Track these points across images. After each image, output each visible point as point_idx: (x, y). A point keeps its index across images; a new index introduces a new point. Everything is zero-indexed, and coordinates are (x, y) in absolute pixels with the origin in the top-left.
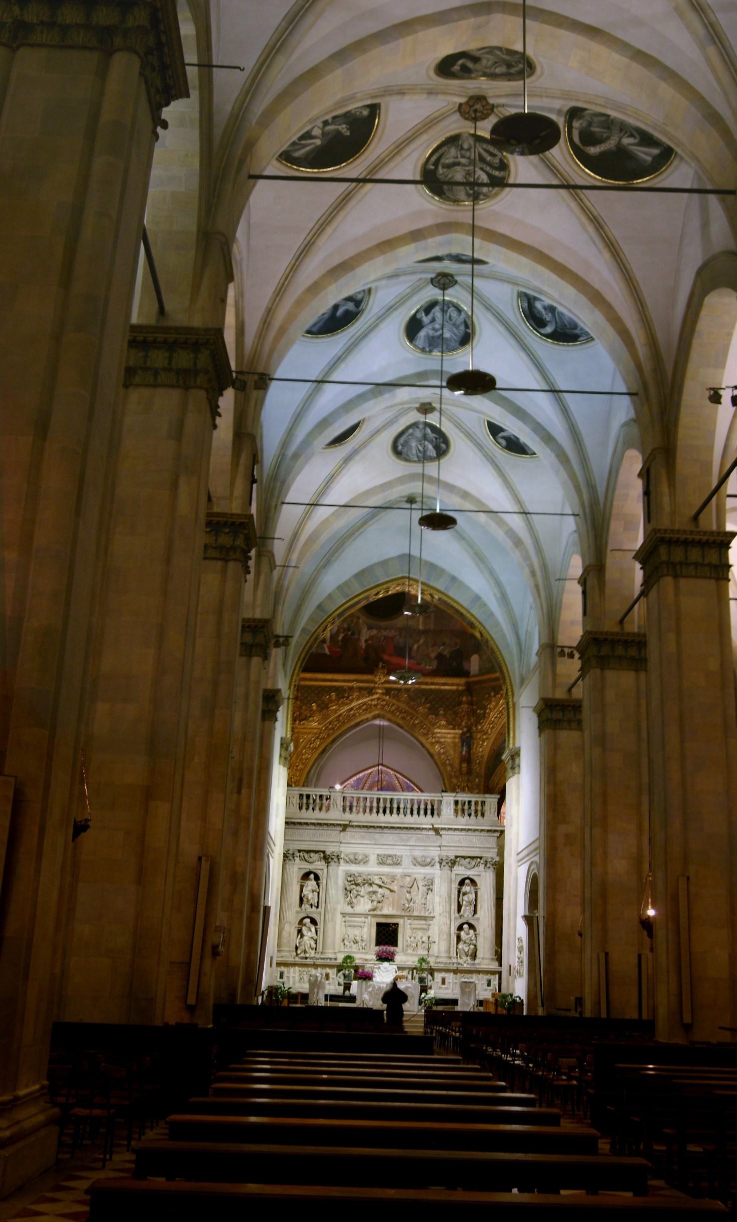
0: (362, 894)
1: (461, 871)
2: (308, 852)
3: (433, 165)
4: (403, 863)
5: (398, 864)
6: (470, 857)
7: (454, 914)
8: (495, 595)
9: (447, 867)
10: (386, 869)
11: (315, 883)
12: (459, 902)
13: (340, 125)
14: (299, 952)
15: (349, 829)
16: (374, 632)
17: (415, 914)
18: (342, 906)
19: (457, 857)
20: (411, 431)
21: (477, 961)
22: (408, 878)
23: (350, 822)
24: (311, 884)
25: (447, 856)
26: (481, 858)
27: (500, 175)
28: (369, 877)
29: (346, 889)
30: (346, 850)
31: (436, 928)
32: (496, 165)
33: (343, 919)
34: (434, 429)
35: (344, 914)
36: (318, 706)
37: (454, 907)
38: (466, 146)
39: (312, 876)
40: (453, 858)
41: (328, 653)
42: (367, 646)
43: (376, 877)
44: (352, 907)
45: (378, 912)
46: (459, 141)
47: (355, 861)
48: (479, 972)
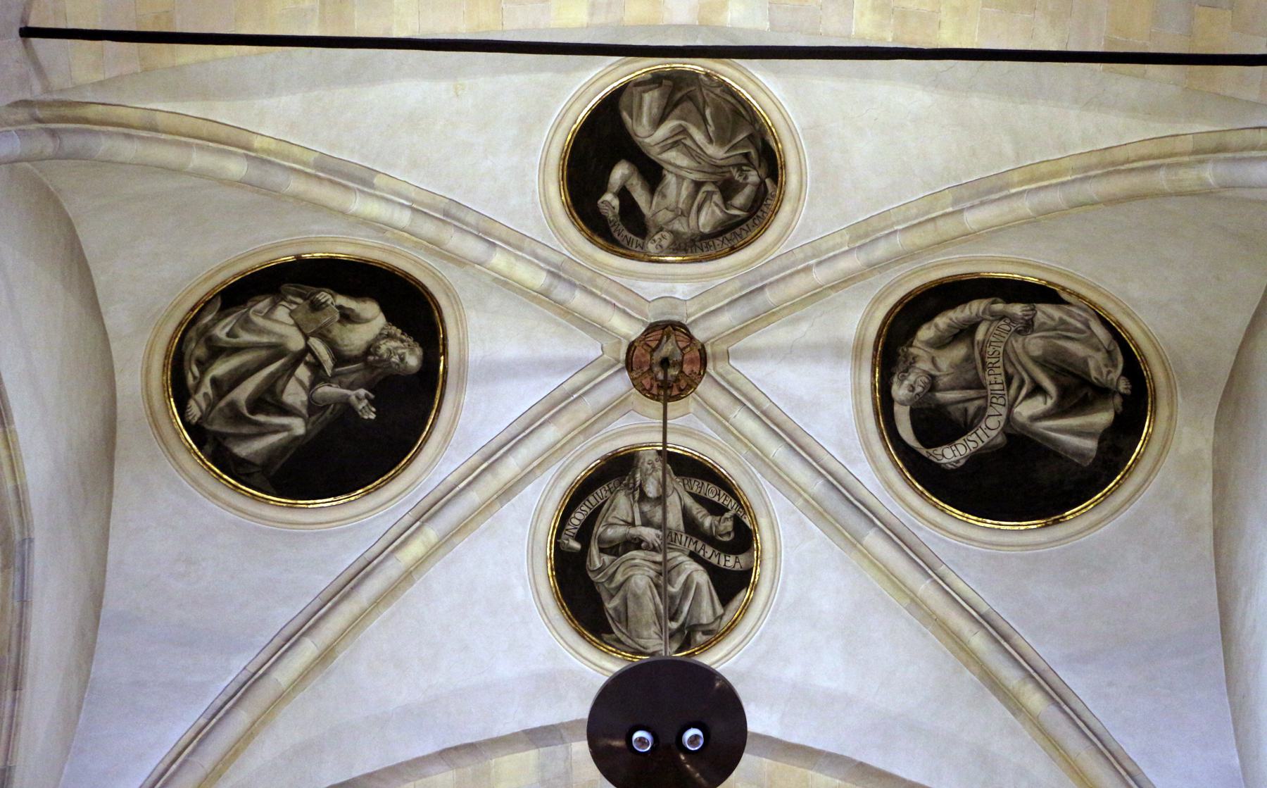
3: (577, 538)
13: (351, 386)
27: (738, 567)
32: (726, 539)
38: (652, 490)
46: (634, 474)
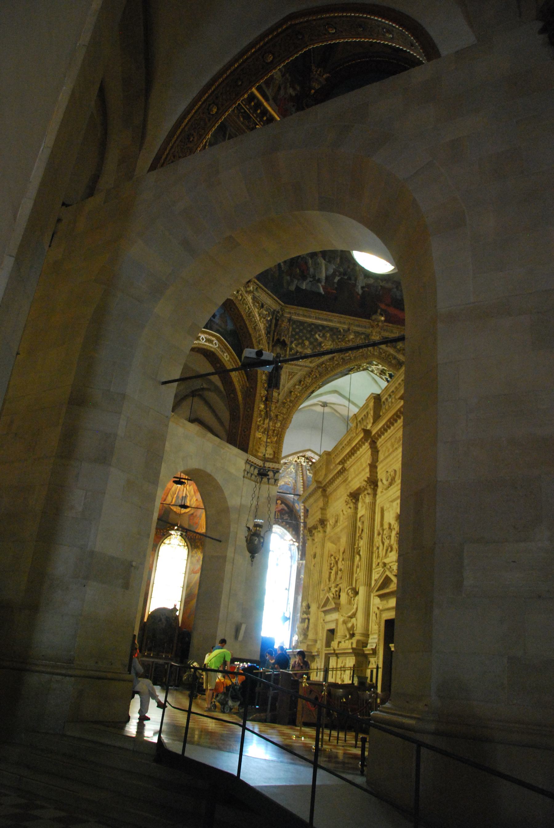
36: (311, 343)
41: (323, 293)
42: (364, 292)
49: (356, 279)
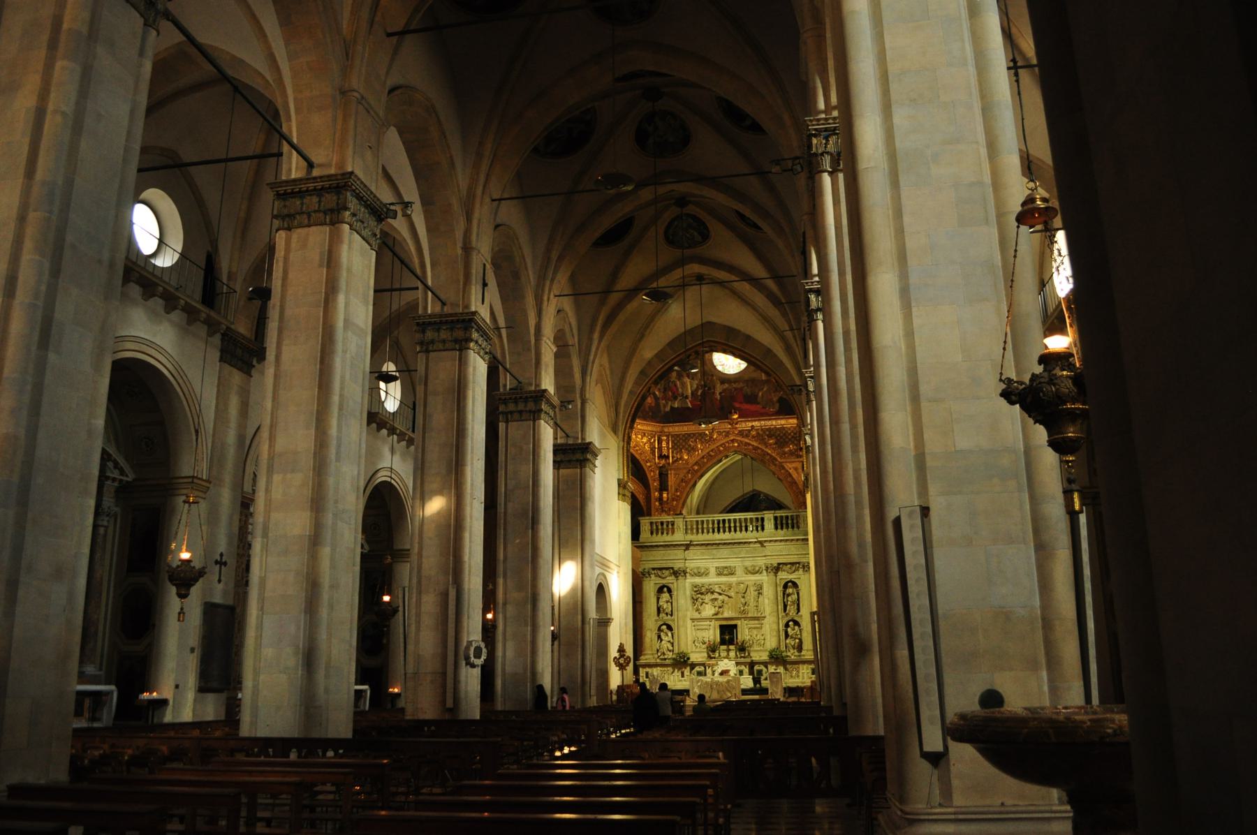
0: (706, 601)
1: (784, 576)
2: (661, 569)
4: (737, 573)
5: (732, 574)
6: (790, 563)
7: (781, 614)
8: (781, 347)
9: (772, 574)
10: (723, 579)
11: (668, 595)
12: (784, 602)
14: (659, 654)
15: (691, 548)
16: (726, 386)
17: (750, 615)
18: (691, 613)
19: (779, 564)
20: (676, 223)
21: (803, 653)
22: (742, 585)
23: (691, 541)
24: (665, 596)
25: (771, 564)
26: (799, 563)
28: (711, 587)
29: (693, 598)
30: (691, 565)
31: (768, 626)
33: (693, 624)
34: (694, 217)
35: (693, 620)
37: (781, 607)
39: (665, 589)
40: (776, 565)
42: (721, 397)
43: (716, 586)
44: (699, 613)
45: (720, 616)
47: (699, 574)
48: (804, 662)
49: (714, 388)
